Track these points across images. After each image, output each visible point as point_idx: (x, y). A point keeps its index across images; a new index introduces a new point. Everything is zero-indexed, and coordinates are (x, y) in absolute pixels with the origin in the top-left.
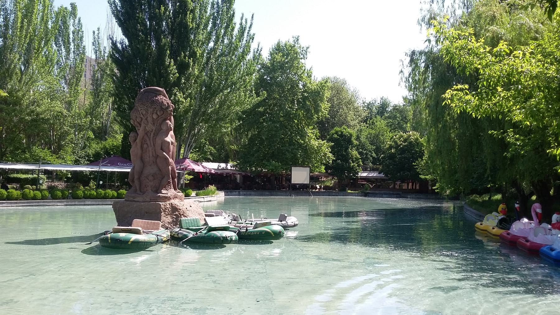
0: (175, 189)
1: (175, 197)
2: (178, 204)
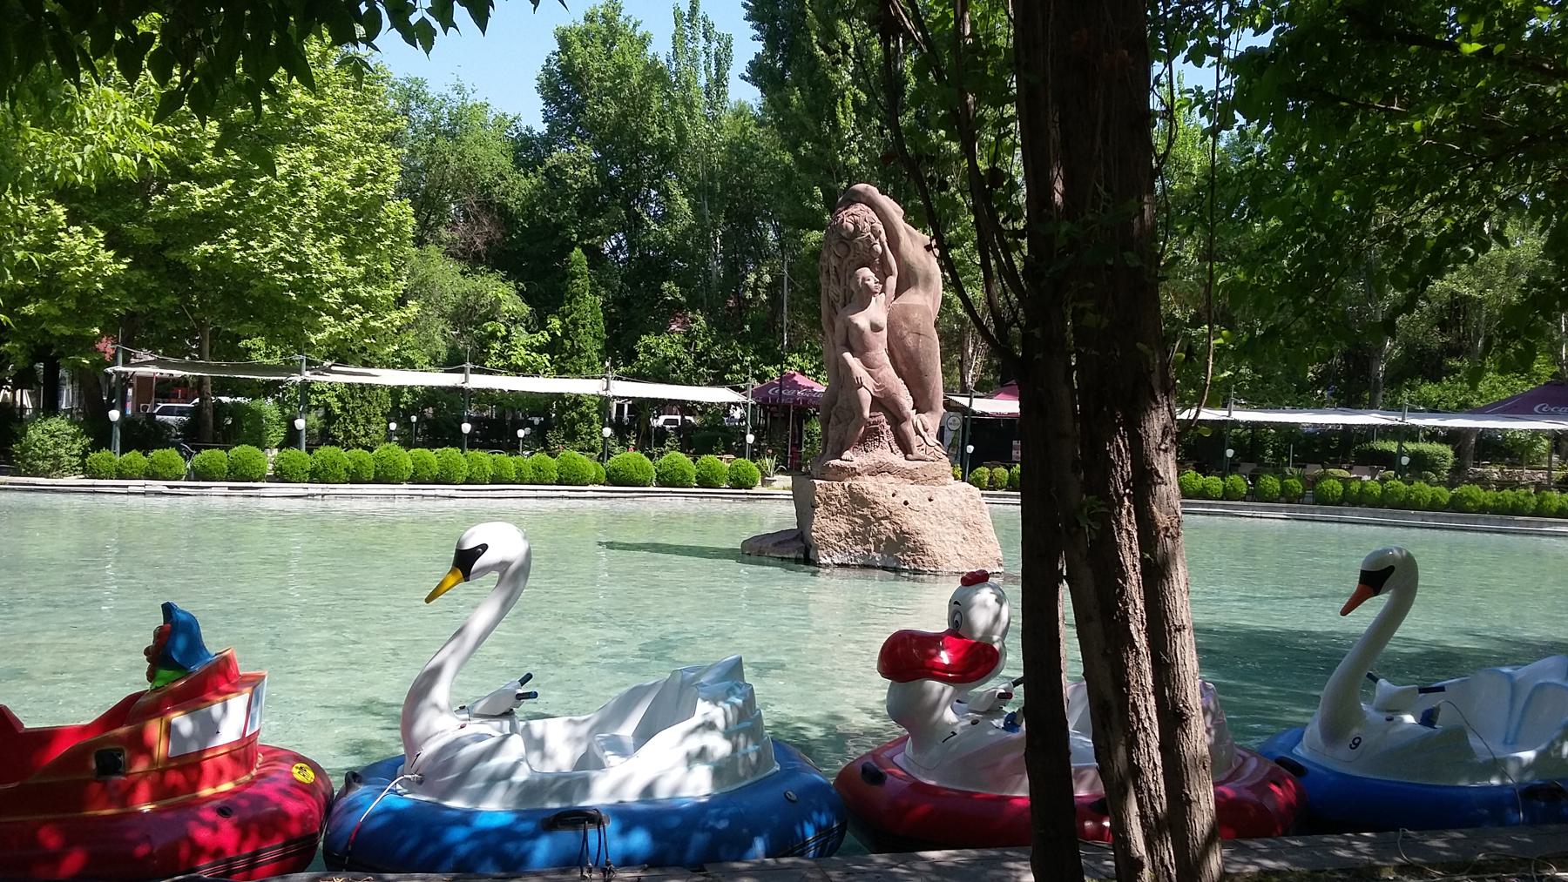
0: (905, 447)
1: (878, 470)
2: (872, 489)
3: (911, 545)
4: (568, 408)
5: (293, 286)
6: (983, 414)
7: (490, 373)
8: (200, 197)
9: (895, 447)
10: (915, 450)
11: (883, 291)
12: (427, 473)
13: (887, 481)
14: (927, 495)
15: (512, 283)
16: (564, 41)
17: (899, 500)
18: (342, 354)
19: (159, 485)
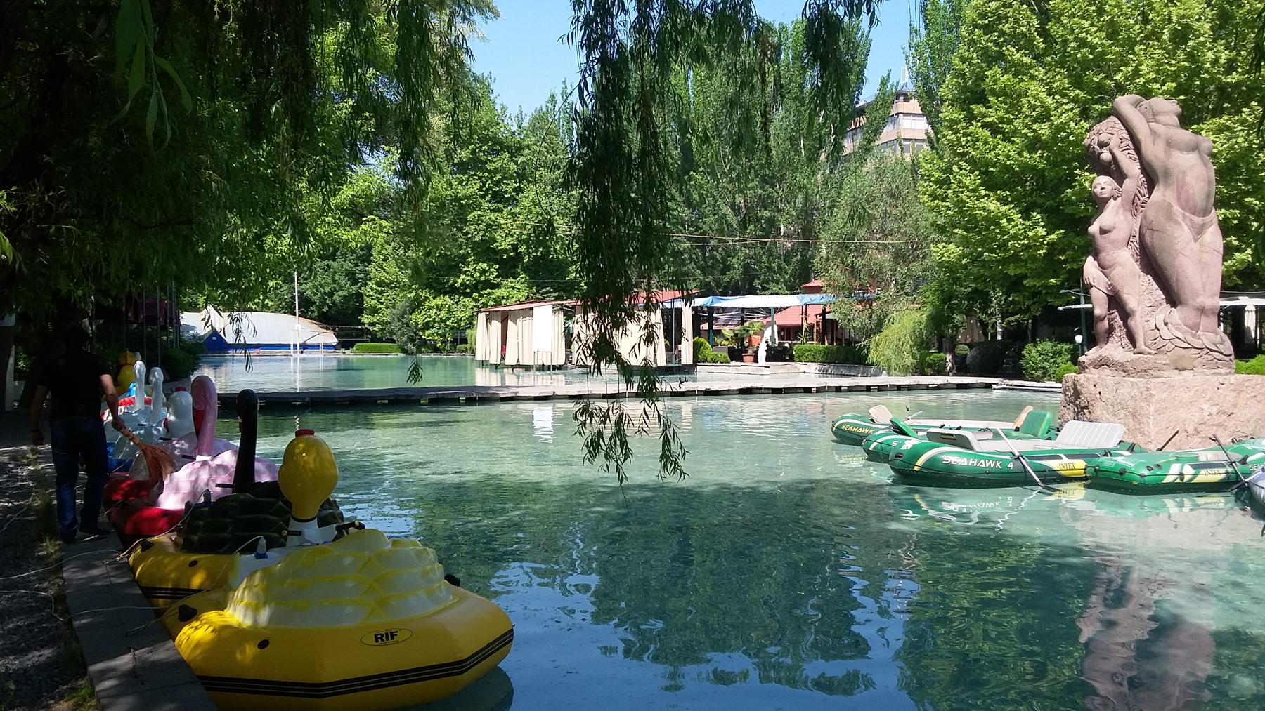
1: (1100, 363)
9: (1126, 341)
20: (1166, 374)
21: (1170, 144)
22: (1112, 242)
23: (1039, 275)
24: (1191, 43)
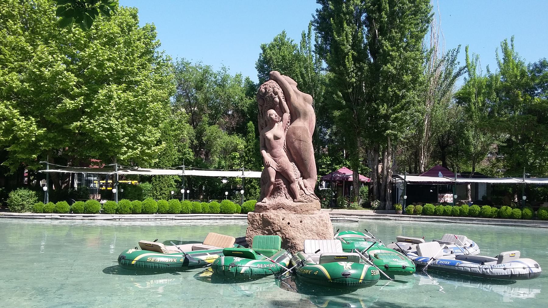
0: (293, 195)
1: (278, 207)
2: (272, 217)
3: (290, 245)
4: (246, 183)
5: (108, 136)
6: (409, 182)
7: (235, 170)
8: (69, 104)
9: (288, 196)
10: (299, 197)
11: (282, 120)
12: (163, 209)
13: (281, 213)
14: (299, 220)
15: (244, 138)
16: (263, 48)
17: (285, 222)
18: (134, 162)
19: (57, 215)
20: (315, 212)
21: (305, 99)
22: (280, 144)
23: (23, 152)
24: (116, 46)
